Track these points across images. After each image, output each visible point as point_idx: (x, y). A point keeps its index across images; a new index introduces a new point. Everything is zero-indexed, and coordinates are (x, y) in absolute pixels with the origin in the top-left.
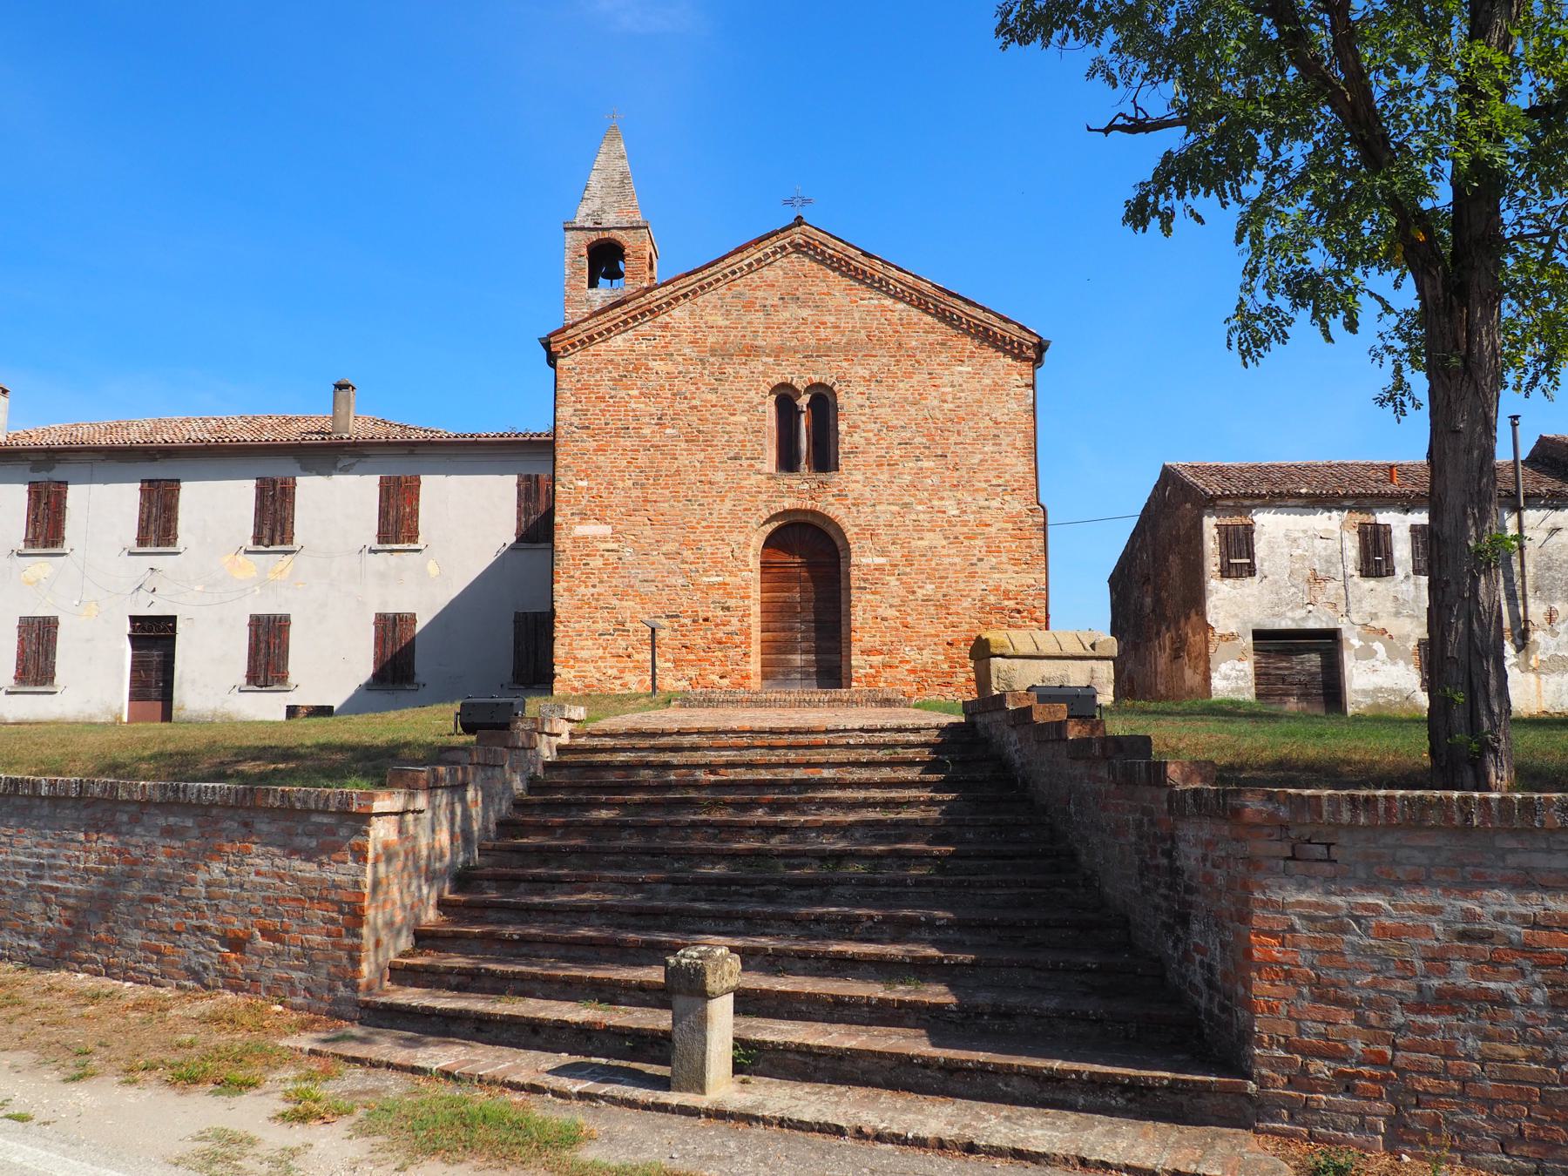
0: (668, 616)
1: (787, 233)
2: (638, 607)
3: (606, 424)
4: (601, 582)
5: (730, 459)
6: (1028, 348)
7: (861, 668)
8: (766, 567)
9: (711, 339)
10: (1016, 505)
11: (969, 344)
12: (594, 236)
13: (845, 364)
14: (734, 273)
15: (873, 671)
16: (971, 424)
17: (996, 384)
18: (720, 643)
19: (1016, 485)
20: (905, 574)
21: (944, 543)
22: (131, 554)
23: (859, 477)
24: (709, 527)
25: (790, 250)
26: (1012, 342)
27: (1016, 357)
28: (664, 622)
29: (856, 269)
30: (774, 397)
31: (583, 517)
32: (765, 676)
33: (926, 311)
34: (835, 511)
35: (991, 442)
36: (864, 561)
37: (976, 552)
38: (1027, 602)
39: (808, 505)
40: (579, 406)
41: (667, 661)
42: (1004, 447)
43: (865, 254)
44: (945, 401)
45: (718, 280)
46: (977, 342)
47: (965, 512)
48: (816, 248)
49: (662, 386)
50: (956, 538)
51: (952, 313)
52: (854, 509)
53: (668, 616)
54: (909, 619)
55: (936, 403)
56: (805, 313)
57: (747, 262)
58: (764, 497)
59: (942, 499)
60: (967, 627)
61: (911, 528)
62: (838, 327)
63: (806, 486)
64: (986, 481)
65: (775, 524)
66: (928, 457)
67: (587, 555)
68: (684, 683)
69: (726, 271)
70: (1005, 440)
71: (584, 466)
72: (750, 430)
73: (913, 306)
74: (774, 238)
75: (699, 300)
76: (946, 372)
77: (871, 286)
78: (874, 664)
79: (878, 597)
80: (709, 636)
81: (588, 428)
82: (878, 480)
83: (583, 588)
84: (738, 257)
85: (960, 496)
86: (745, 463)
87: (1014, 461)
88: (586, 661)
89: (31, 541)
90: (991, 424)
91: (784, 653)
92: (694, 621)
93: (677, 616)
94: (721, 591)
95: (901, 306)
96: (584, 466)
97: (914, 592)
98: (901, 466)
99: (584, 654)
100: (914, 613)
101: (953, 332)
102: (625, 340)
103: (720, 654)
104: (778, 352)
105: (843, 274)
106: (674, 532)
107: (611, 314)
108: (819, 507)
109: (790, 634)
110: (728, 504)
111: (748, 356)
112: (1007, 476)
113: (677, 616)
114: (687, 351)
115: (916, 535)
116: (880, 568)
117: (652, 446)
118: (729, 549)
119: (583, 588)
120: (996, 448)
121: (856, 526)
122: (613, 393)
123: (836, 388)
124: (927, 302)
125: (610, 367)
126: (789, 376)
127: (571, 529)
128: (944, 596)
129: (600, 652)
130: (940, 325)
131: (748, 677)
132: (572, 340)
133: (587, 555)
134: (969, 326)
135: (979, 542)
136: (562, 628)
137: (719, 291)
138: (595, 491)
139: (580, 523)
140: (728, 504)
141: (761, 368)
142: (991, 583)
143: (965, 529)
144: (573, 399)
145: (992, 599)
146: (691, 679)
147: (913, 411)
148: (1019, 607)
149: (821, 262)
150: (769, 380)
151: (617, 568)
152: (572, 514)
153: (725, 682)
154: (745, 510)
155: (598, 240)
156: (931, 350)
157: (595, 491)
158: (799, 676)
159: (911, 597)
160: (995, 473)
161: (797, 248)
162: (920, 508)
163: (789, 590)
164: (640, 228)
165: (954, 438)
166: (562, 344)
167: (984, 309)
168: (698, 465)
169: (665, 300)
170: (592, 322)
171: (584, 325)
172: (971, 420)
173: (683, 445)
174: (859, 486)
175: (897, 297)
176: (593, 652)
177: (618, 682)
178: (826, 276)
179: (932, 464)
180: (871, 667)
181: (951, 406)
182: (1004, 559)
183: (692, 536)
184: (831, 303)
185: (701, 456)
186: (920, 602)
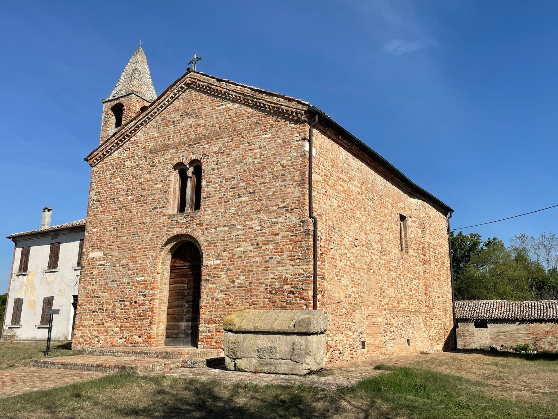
0: (120, 301)
1: (183, 79)
2: (109, 296)
3: (107, 197)
4: (96, 283)
5: (153, 209)
6: (302, 115)
7: (204, 332)
8: (173, 268)
9: (151, 145)
10: (293, 220)
11: (271, 120)
12: (113, 103)
13: (207, 146)
14: (161, 107)
15: (210, 334)
16: (269, 170)
17: (284, 142)
18: (140, 316)
19: (294, 206)
20: (229, 270)
21: (251, 248)
22: (75, 270)
23: (210, 212)
24: (141, 248)
25: (186, 88)
26: (292, 112)
27: (298, 122)
28: (118, 304)
29: (214, 89)
30: (177, 171)
31: (93, 247)
32: (168, 336)
33: (248, 106)
34: (197, 234)
35: (280, 180)
36: (210, 263)
37: (269, 253)
38: (298, 286)
39: (185, 231)
40: (97, 190)
41: (117, 327)
42: (288, 182)
43: (219, 80)
44: (256, 158)
45: (155, 113)
46: (275, 118)
47: (263, 227)
48: (196, 83)
49: (129, 174)
50: (258, 244)
51: (260, 103)
52: (206, 231)
53: (120, 301)
54: (230, 300)
55: (251, 160)
56: (191, 121)
57: (167, 100)
58: (165, 229)
59: (251, 220)
60: (262, 304)
61: (234, 240)
62: (206, 125)
63: (185, 220)
64: (276, 205)
65: (172, 244)
66: (245, 194)
67: (93, 268)
68: (123, 340)
69: (158, 107)
70: (288, 177)
71: (96, 221)
72: (163, 191)
73: (242, 104)
74: (178, 83)
75: (148, 126)
76: (257, 140)
77: (221, 98)
78: (211, 329)
79: (215, 286)
80: (136, 312)
81: (99, 201)
82: (219, 212)
83: (89, 287)
84: (162, 99)
85: (261, 216)
86: (159, 210)
87: (293, 190)
88: (86, 327)
89: (49, 267)
90: (281, 168)
91: (177, 321)
92: (131, 303)
93: (124, 301)
94: (143, 286)
95: (236, 105)
96: (96, 221)
97: (234, 282)
98: (231, 202)
99: (86, 323)
100: (233, 296)
101: (262, 115)
102: (118, 153)
103: (139, 323)
104: (177, 146)
105: (210, 95)
106: (127, 253)
107: (111, 141)
108: (189, 232)
109: (180, 309)
110: (150, 235)
111: (165, 150)
112: (288, 201)
113: (124, 301)
114: (140, 153)
115: (236, 245)
116: (216, 267)
117: (122, 207)
118: (148, 261)
119: (89, 287)
120: (283, 183)
121: (206, 241)
122: (110, 181)
123: (202, 161)
124: (248, 100)
125: (110, 168)
126: (182, 158)
127: (88, 255)
128: (250, 283)
129: (92, 321)
130: (256, 112)
131: (150, 337)
132: (97, 157)
133: (93, 268)
134: (270, 109)
135: (271, 246)
136: (79, 308)
137: (157, 118)
138: (99, 234)
139: (92, 251)
140: (150, 235)
141: (169, 156)
142: (277, 273)
143: (263, 238)
144: (96, 187)
145: (277, 285)
146: (126, 338)
147: (239, 168)
148: (293, 289)
149: (199, 91)
150: (172, 162)
151: (102, 275)
152: (89, 247)
153: (141, 339)
154: (157, 237)
155: (115, 105)
156: (250, 128)
157: (99, 234)
158: (183, 336)
159: (232, 285)
160: (281, 200)
161: (188, 85)
162: (239, 227)
163: (182, 282)
164: (129, 94)
165: (260, 180)
166: (92, 160)
167: (277, 96)
168: (139, 214)
169: (133, 128)
170: (104, 147)
171: (101, 149)
172: (270, 167)
173: (135, 204)
174: (209, 217)
175: (234, 101)
176: (89, 322)
177: (97, 339)
178: (202, 98)
179: (247, 198)
180: (209, 332)
181: (259, 160)
182: (285, 257)
183: (133, 254)
184: (203, 112)
185: (141, 209)
186: (236, 288)
